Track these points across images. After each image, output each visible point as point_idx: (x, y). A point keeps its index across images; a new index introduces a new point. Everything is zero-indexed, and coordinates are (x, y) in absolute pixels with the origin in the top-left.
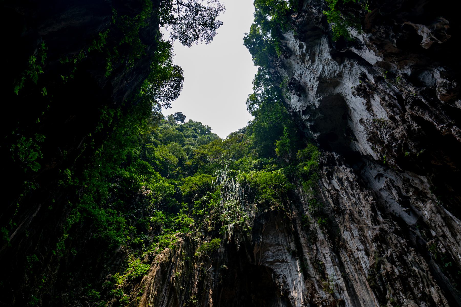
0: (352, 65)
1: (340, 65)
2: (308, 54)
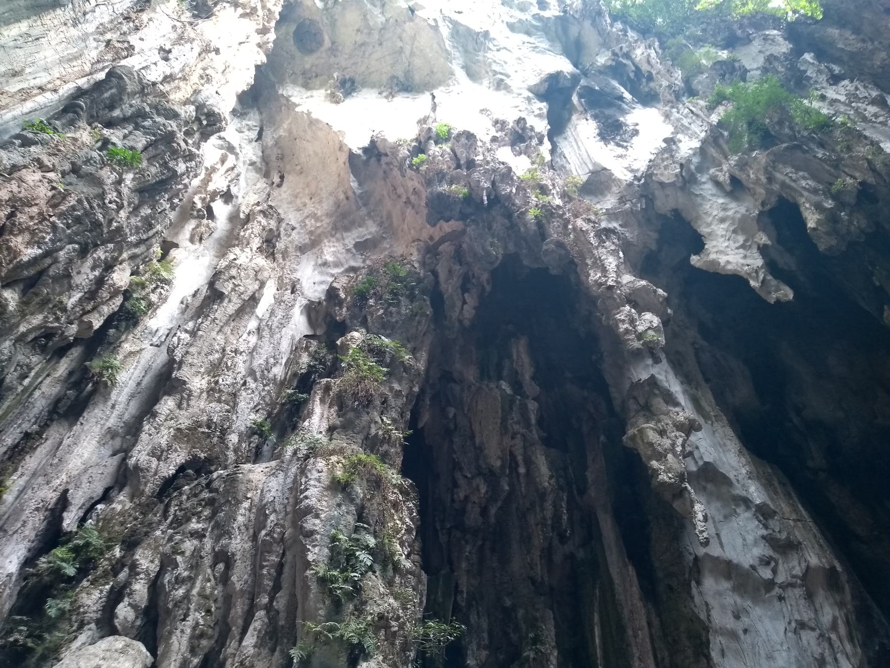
0: (540, 116)
1: (530, 89)
2: (530, 18)
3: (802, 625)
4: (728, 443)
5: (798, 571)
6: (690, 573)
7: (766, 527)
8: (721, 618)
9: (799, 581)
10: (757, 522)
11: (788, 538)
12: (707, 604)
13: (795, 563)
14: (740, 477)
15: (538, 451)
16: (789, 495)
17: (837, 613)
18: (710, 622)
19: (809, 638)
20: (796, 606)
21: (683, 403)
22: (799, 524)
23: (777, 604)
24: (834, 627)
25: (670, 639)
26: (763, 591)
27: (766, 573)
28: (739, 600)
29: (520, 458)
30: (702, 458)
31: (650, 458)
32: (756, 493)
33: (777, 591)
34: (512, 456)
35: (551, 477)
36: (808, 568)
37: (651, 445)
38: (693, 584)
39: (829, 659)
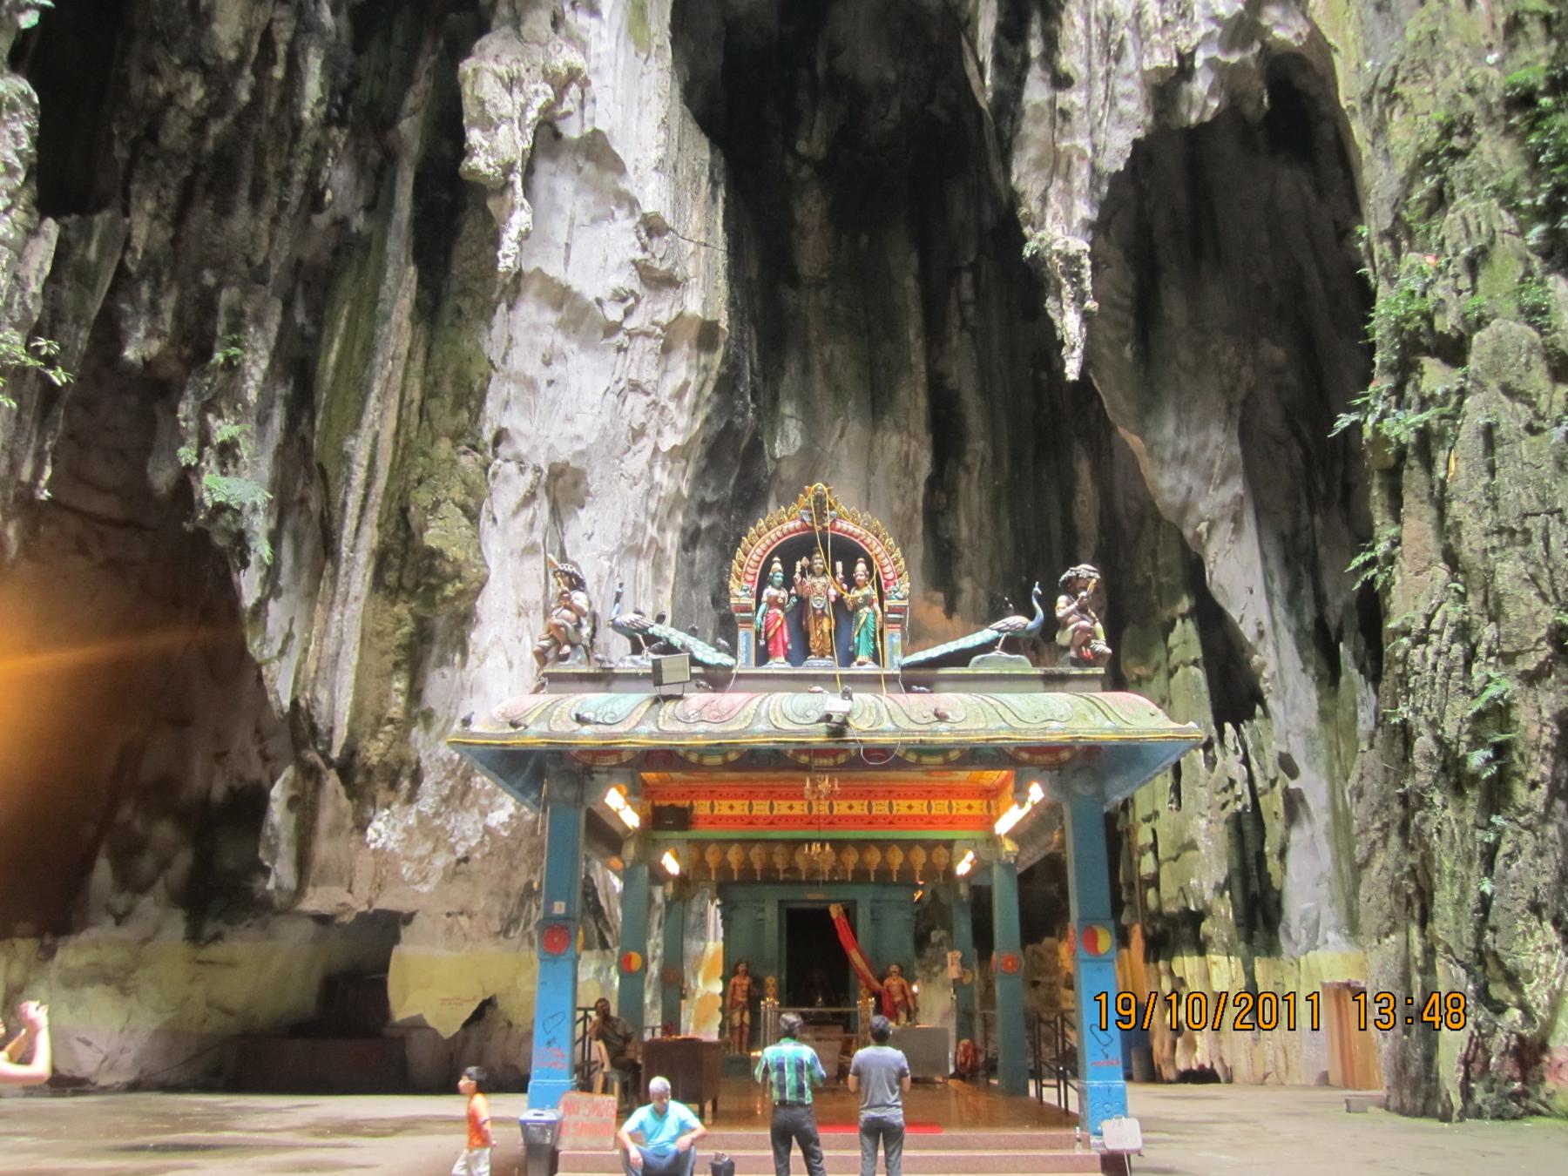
3: (635, 386)
4: (655, 99)
5: (664, 317)
6: (503, 292)
7: (644, 248)
8: (524, 361)
9: (658, 331)
10: (634, 238)
11: (670, 270)
12: (510, 339)
13: (666, 306)
14: (642, 166)
15: (312, 49)
16: (715, 199)
17: (692, 379)
18: (504, 360)
19: (637, 402)
20: (641, 362)
21: (605, 15)
22: (703, 250)
23: (612, 354)
24: (679, 395)
25: (430, 378)
26: (600, 334)
27: (614, 313)
28: (559, 339)
29: (281, 49)
30: (593, 120)
31: (473, 124)
32: (653, 195)
33: (621, 337)
34: (267, 40)
35: (320, 102)
36: (680, 315)
37: (482, 102)
38: (503, 307)
39: (651, 431)
